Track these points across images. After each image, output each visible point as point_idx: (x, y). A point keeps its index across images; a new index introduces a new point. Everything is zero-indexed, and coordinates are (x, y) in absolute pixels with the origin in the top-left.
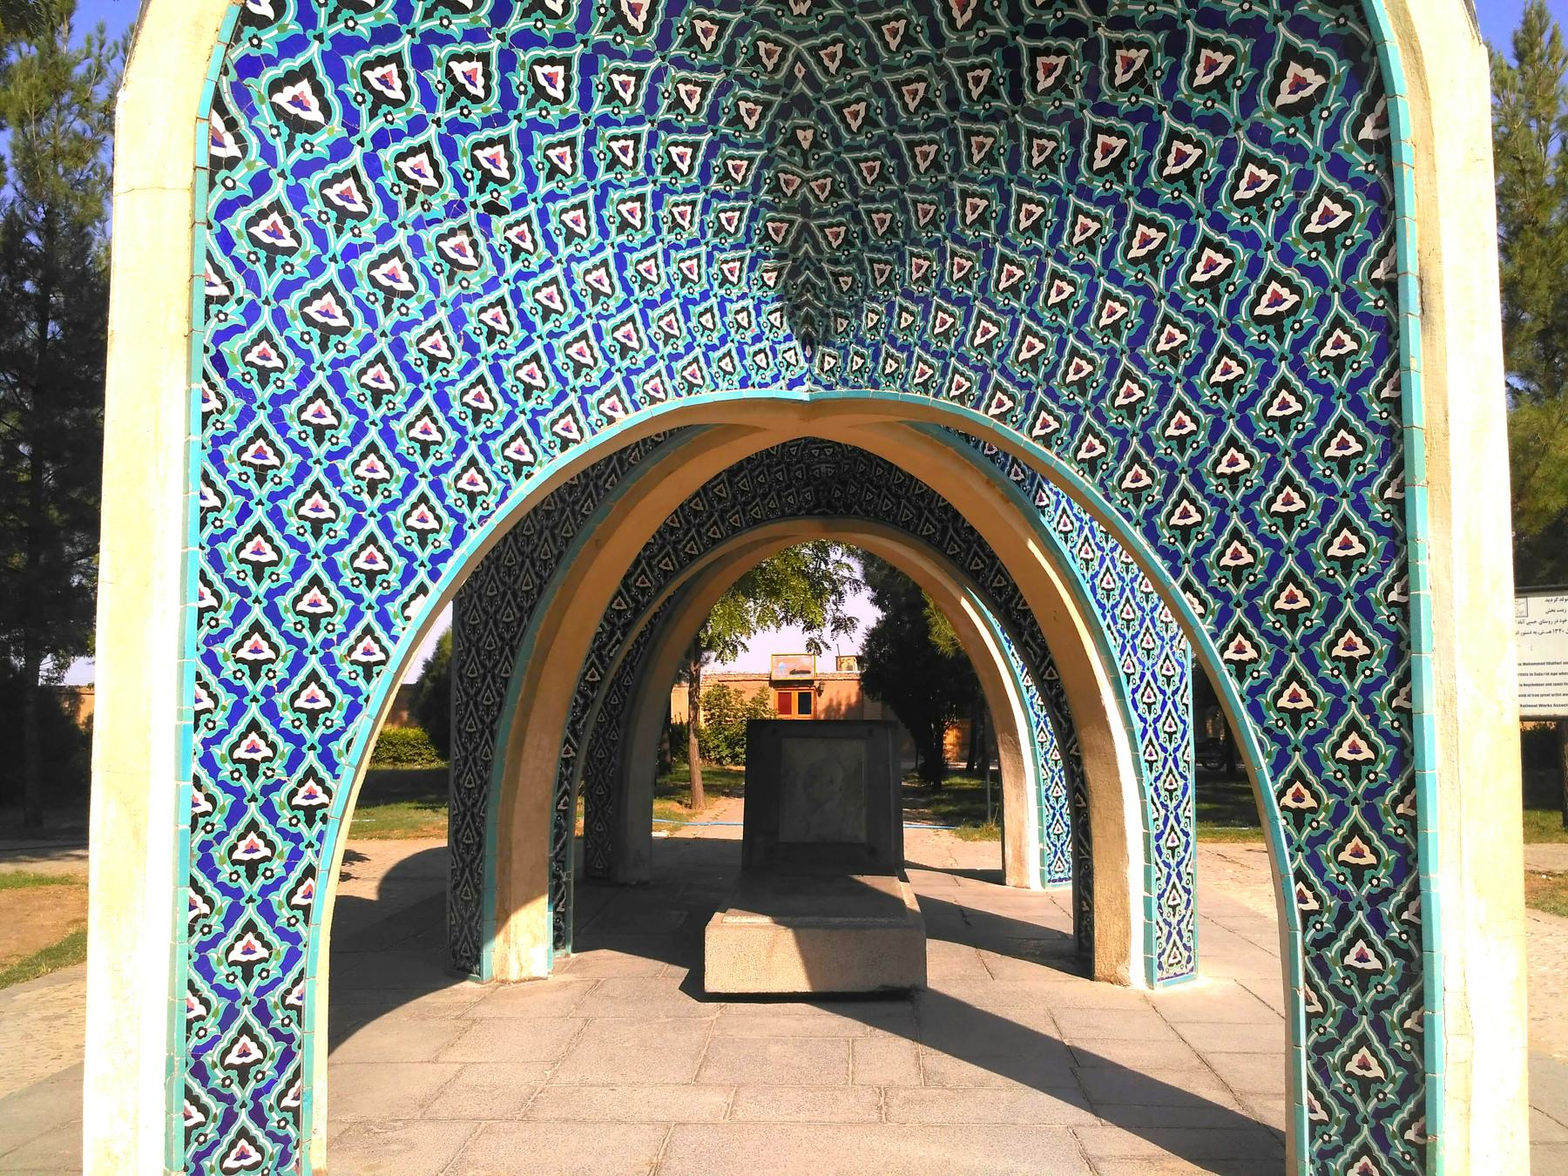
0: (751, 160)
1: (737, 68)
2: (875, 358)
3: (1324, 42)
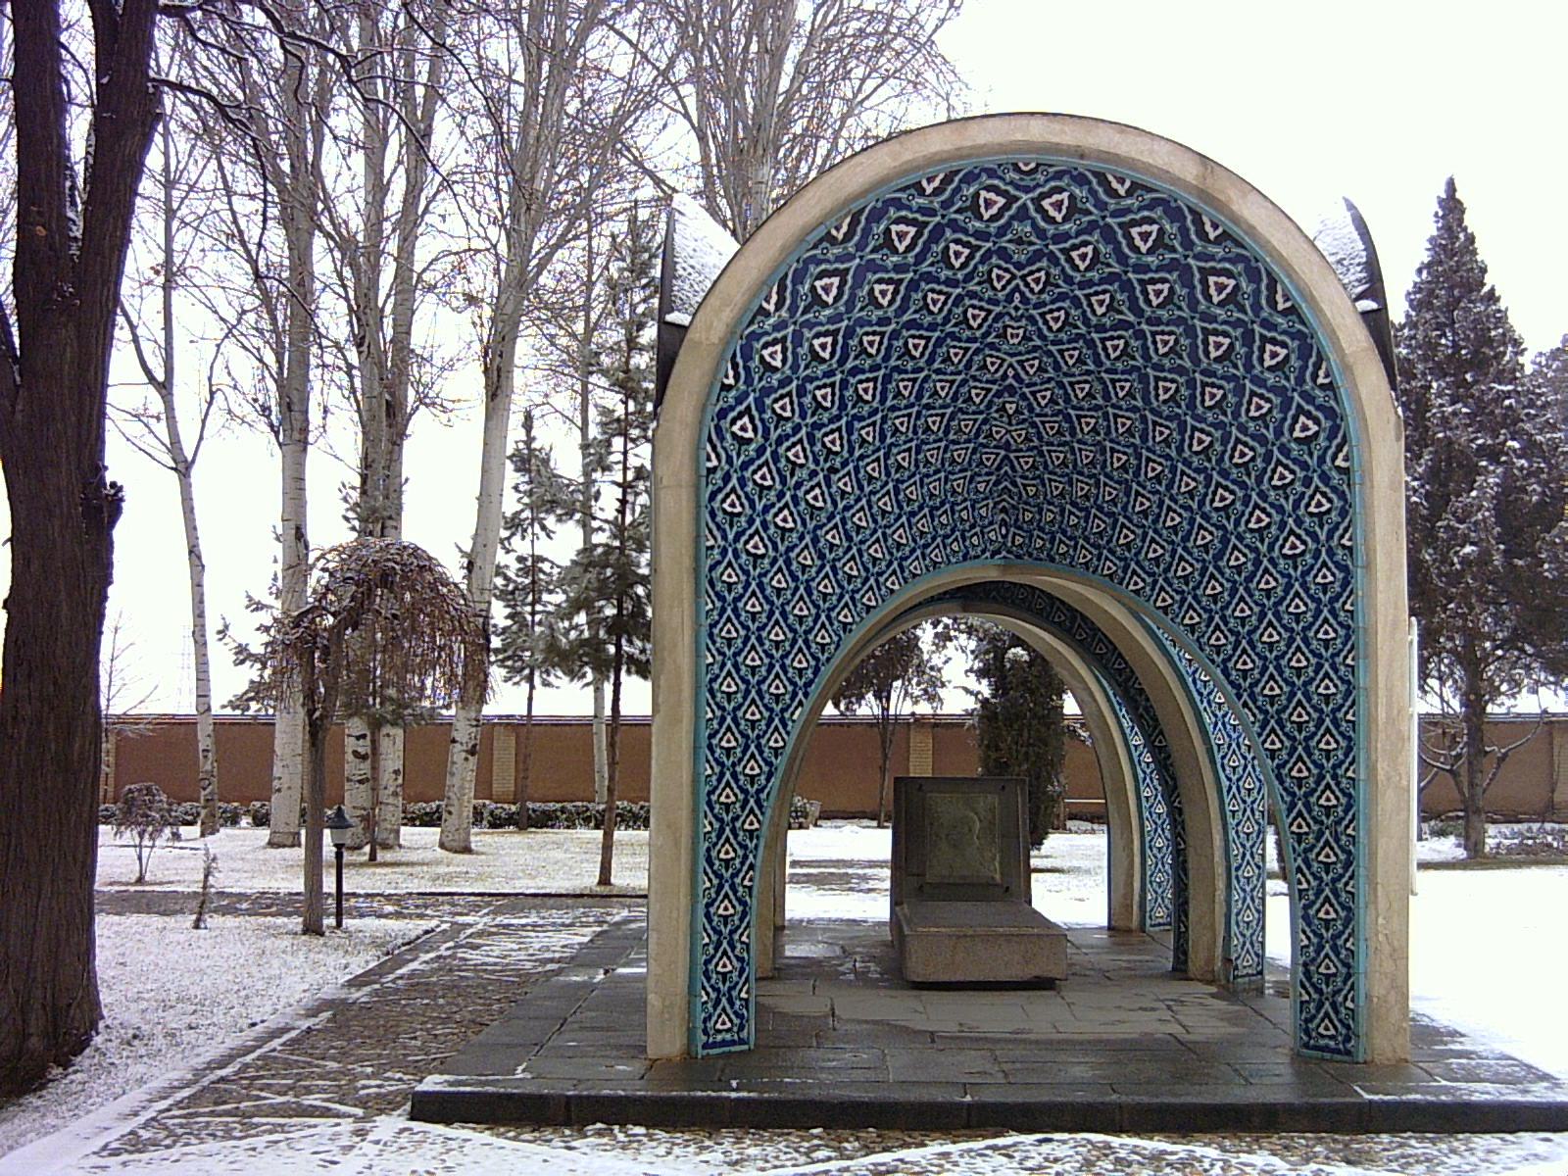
1: (973, 372)
2: (1052, 542)
3: (1318, 408)
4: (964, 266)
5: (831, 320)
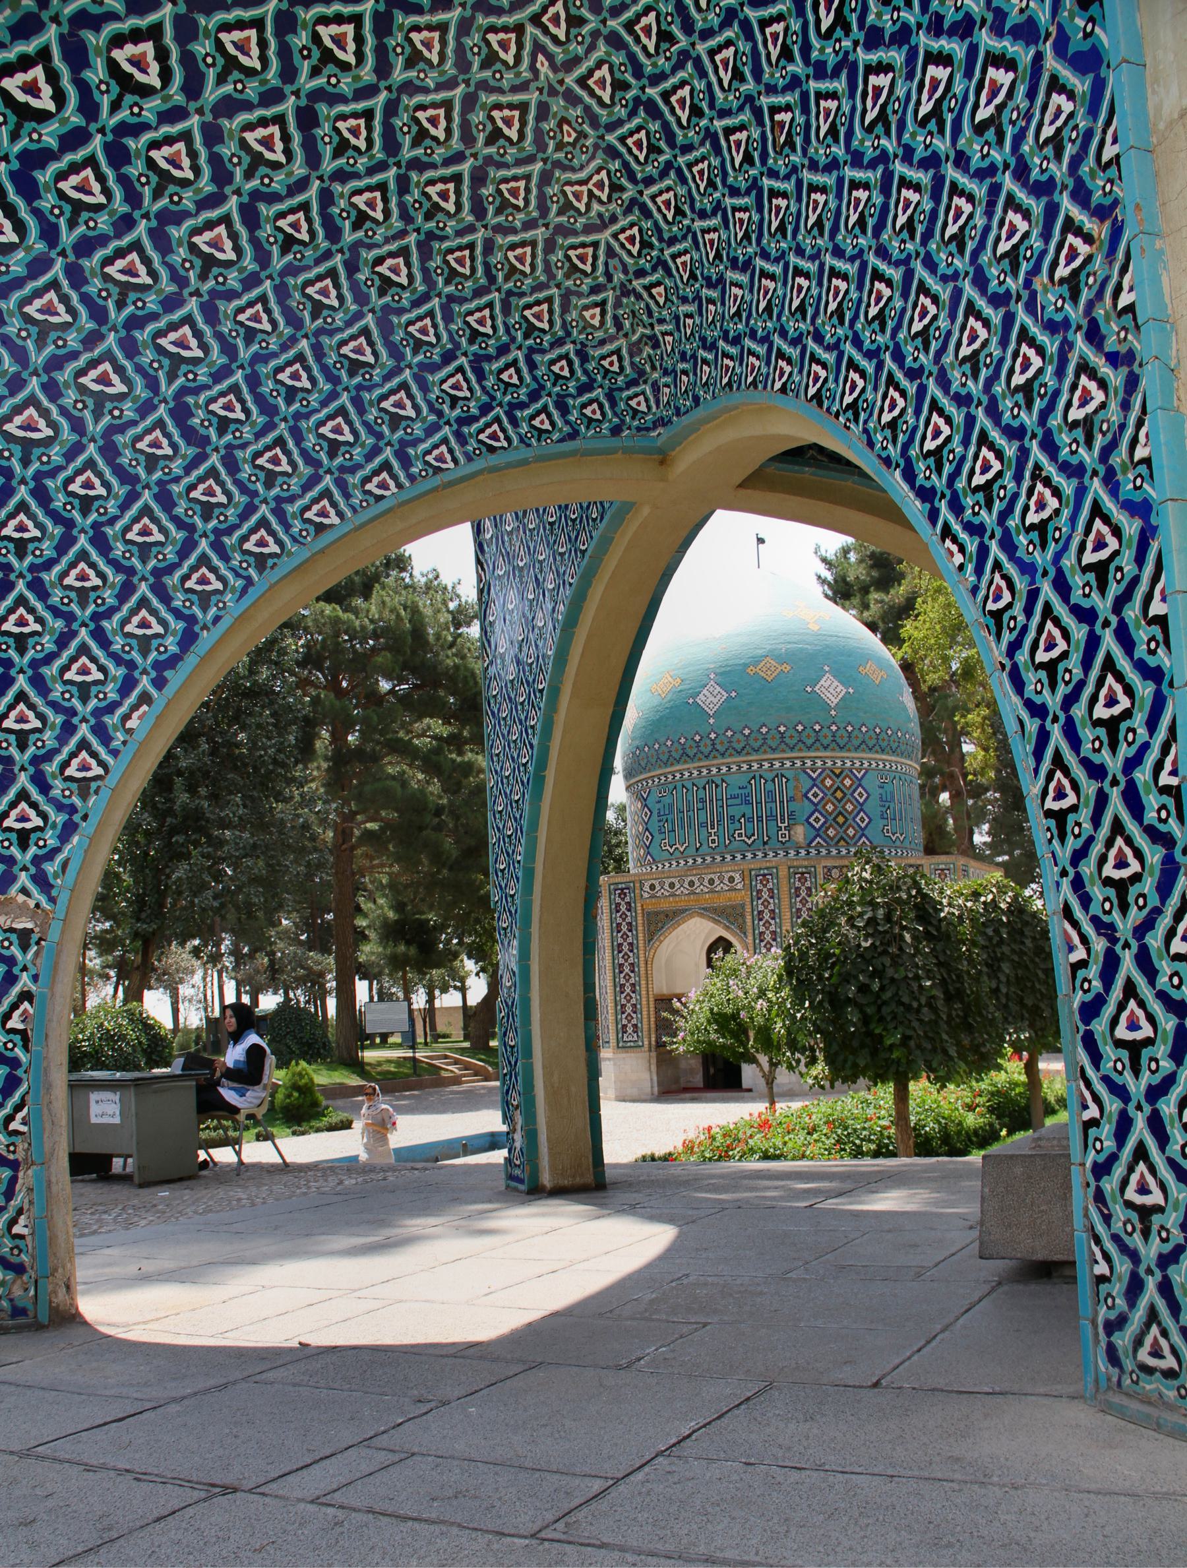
0: (527, 178)
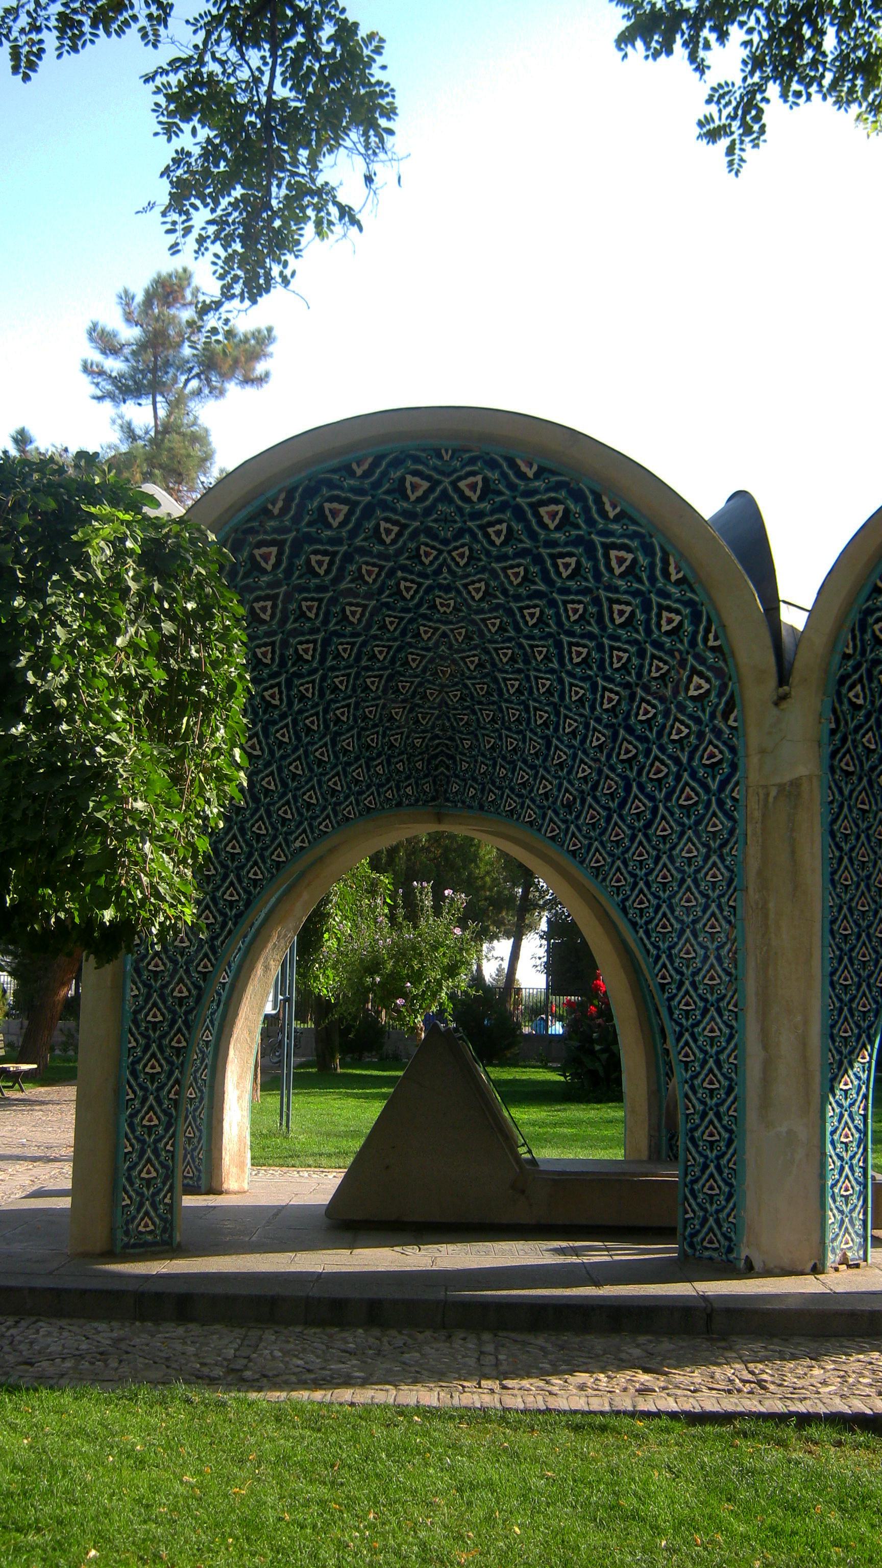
4: (394, 542)
5: (270, 585)
